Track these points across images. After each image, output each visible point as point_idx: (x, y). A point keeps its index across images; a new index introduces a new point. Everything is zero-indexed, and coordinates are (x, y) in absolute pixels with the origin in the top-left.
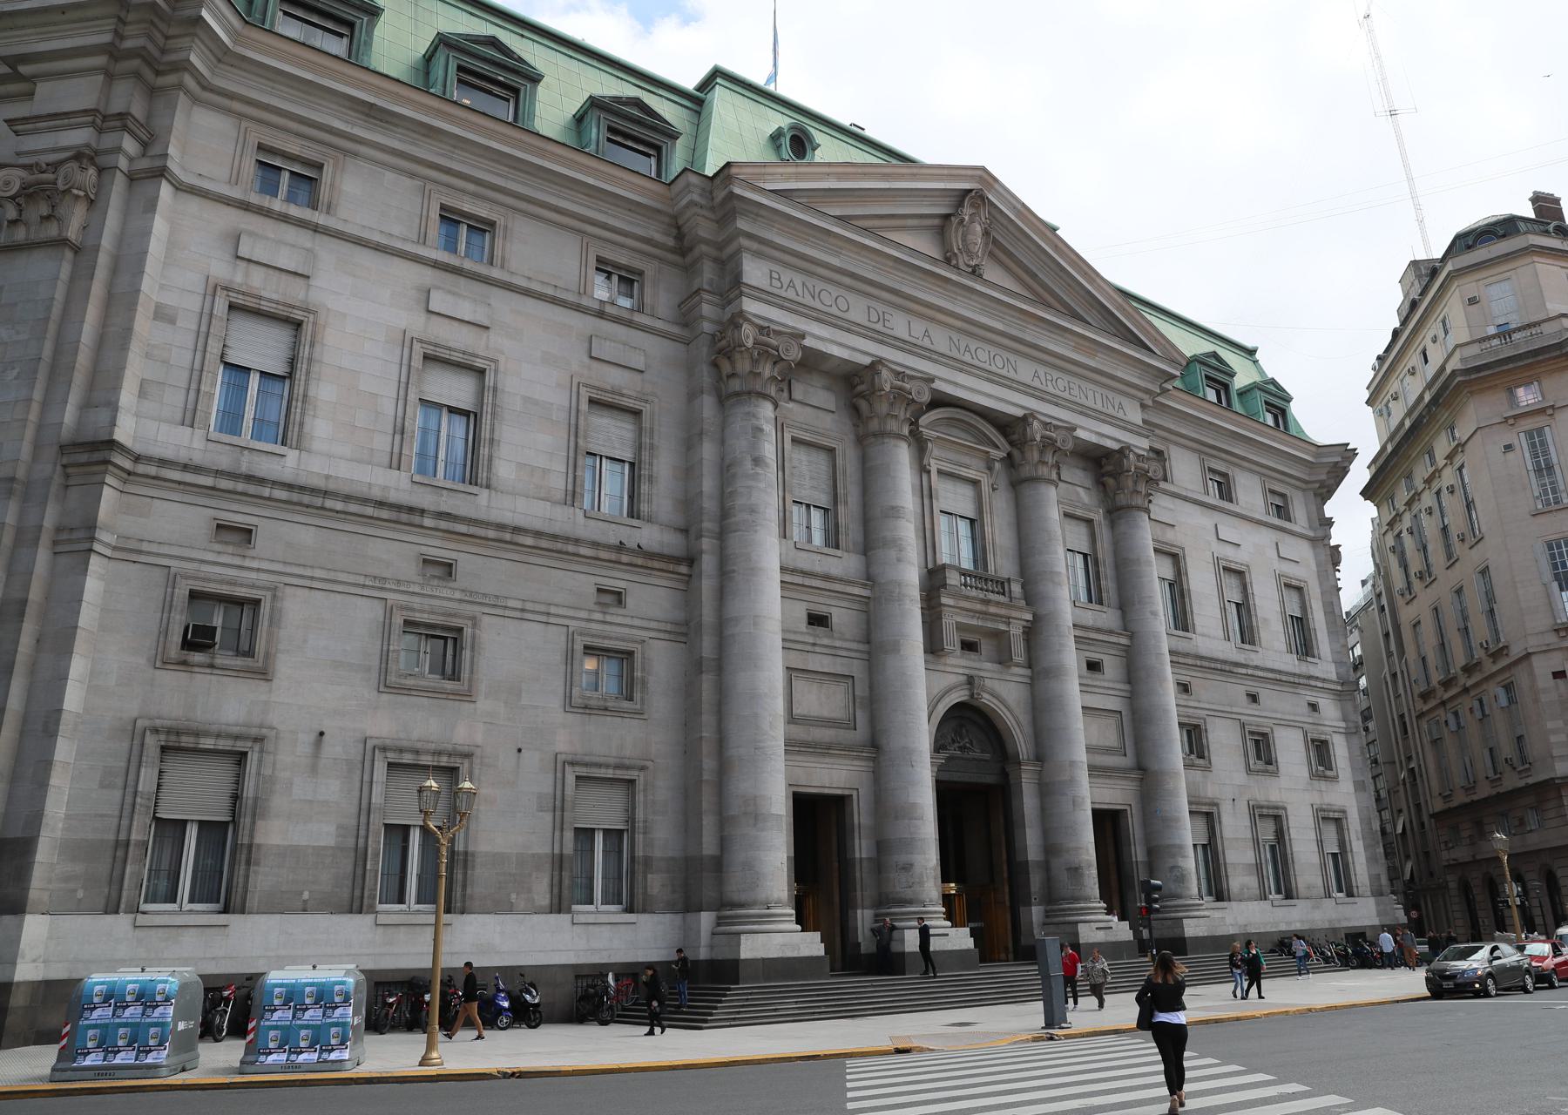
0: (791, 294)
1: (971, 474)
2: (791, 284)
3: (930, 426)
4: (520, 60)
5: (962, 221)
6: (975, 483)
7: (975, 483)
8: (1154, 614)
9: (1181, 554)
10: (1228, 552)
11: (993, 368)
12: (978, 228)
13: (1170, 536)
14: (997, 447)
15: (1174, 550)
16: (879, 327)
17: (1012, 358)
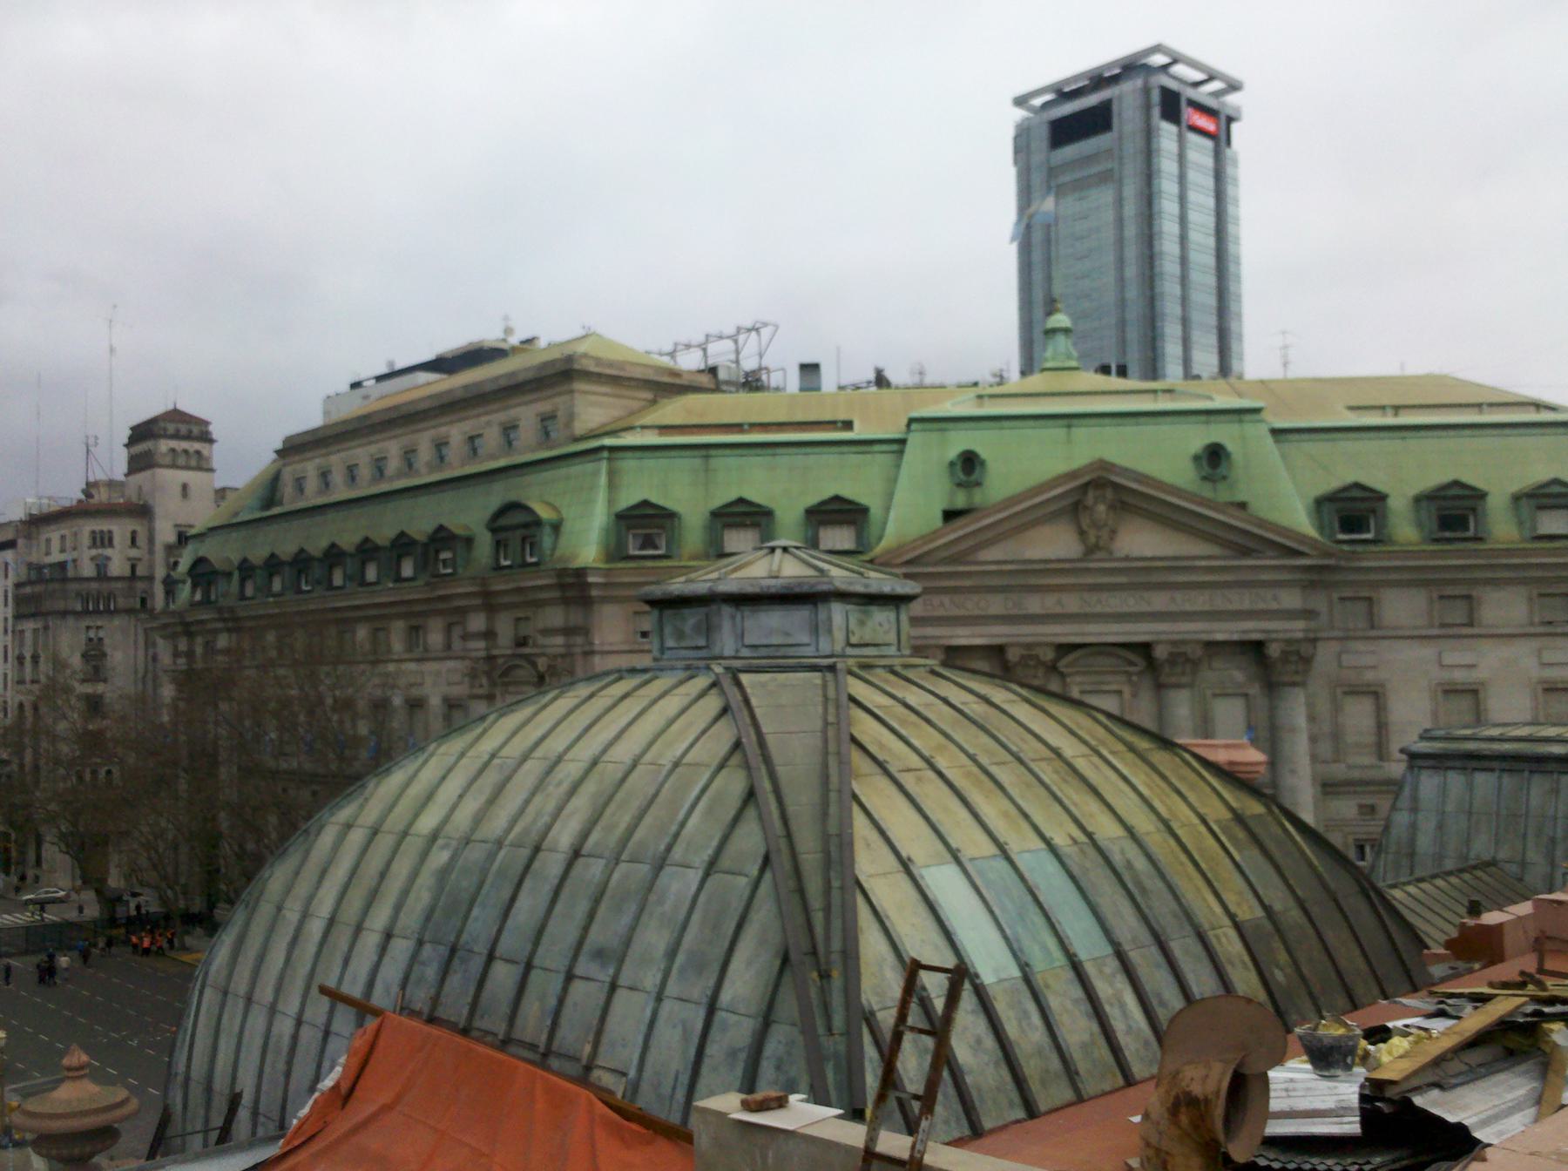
0: (940, 612)
1: (1114, 687)
2: (942, 604)
3: (1067, 666)
4: (759, 506)
5: (1086, 508)
6: (1119, 692)
7: (1119, 692)
8: (1293, 772)
9: (1380, 690)
10: (1460, 676)
11: (1125, 609)
12: (1101, 508)
13: (1369, 676)
14: (1136, 665)
15: (1373, 689)
16: (1015, 611)
17: (1146, 595)
